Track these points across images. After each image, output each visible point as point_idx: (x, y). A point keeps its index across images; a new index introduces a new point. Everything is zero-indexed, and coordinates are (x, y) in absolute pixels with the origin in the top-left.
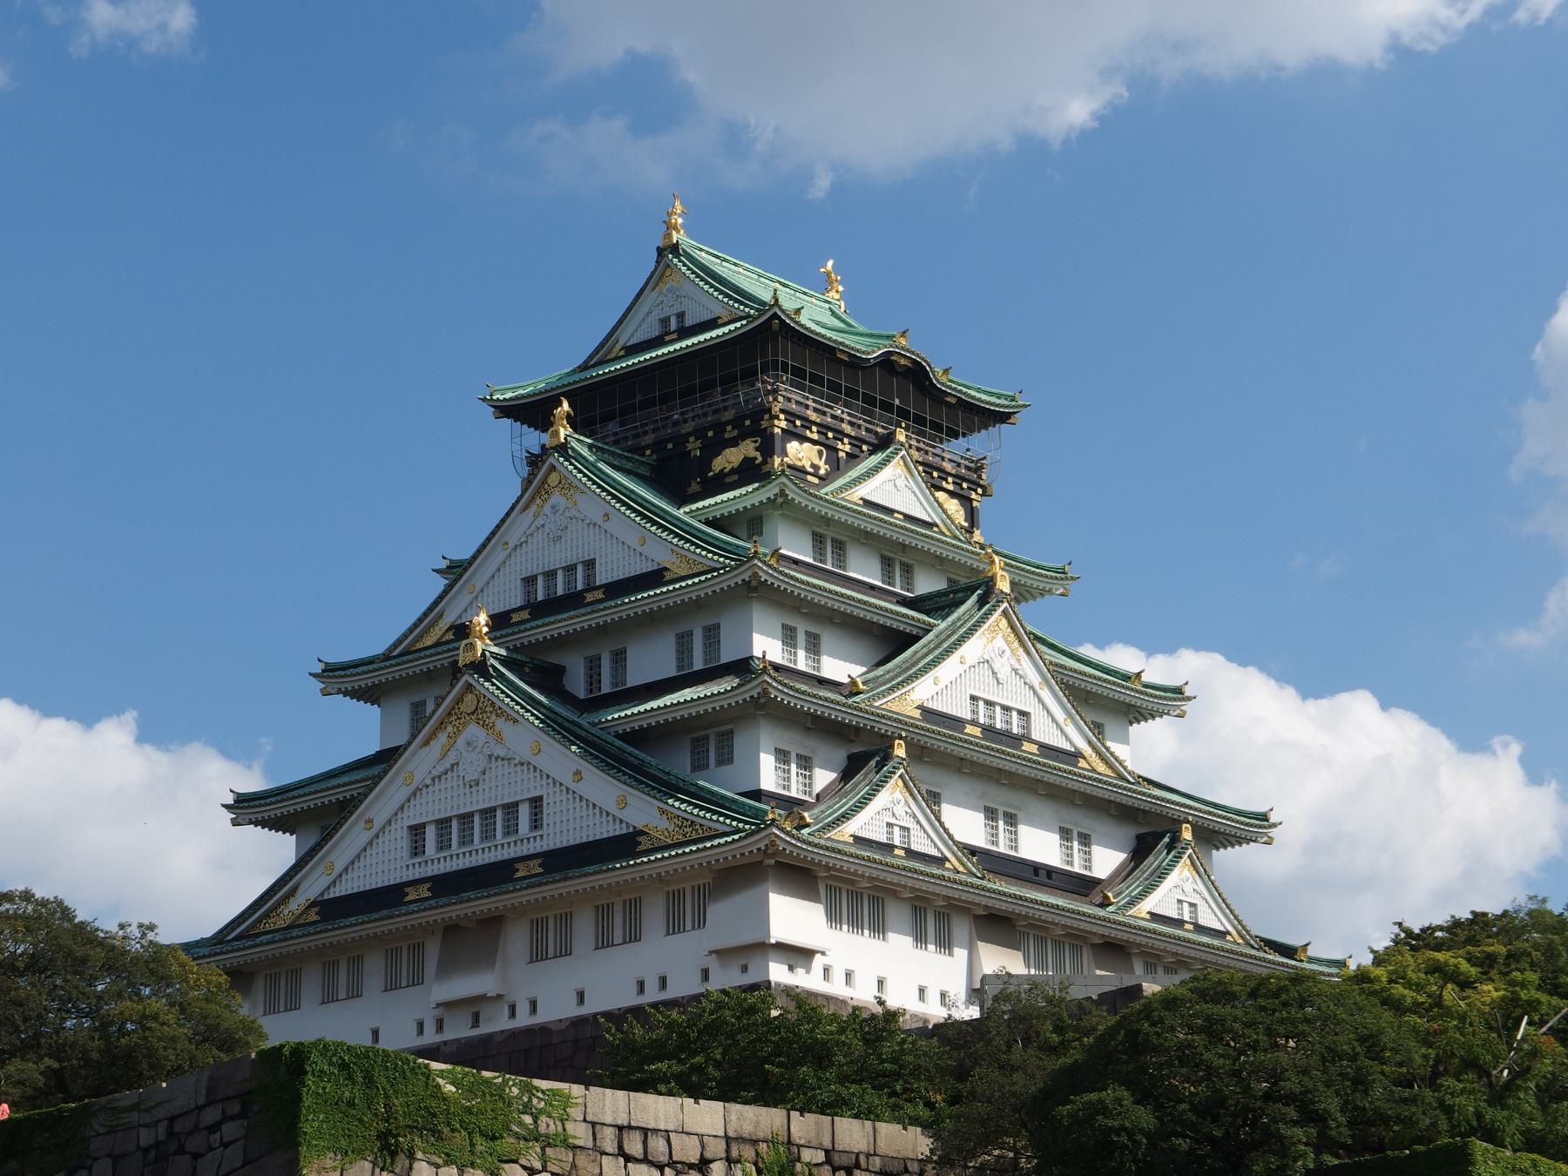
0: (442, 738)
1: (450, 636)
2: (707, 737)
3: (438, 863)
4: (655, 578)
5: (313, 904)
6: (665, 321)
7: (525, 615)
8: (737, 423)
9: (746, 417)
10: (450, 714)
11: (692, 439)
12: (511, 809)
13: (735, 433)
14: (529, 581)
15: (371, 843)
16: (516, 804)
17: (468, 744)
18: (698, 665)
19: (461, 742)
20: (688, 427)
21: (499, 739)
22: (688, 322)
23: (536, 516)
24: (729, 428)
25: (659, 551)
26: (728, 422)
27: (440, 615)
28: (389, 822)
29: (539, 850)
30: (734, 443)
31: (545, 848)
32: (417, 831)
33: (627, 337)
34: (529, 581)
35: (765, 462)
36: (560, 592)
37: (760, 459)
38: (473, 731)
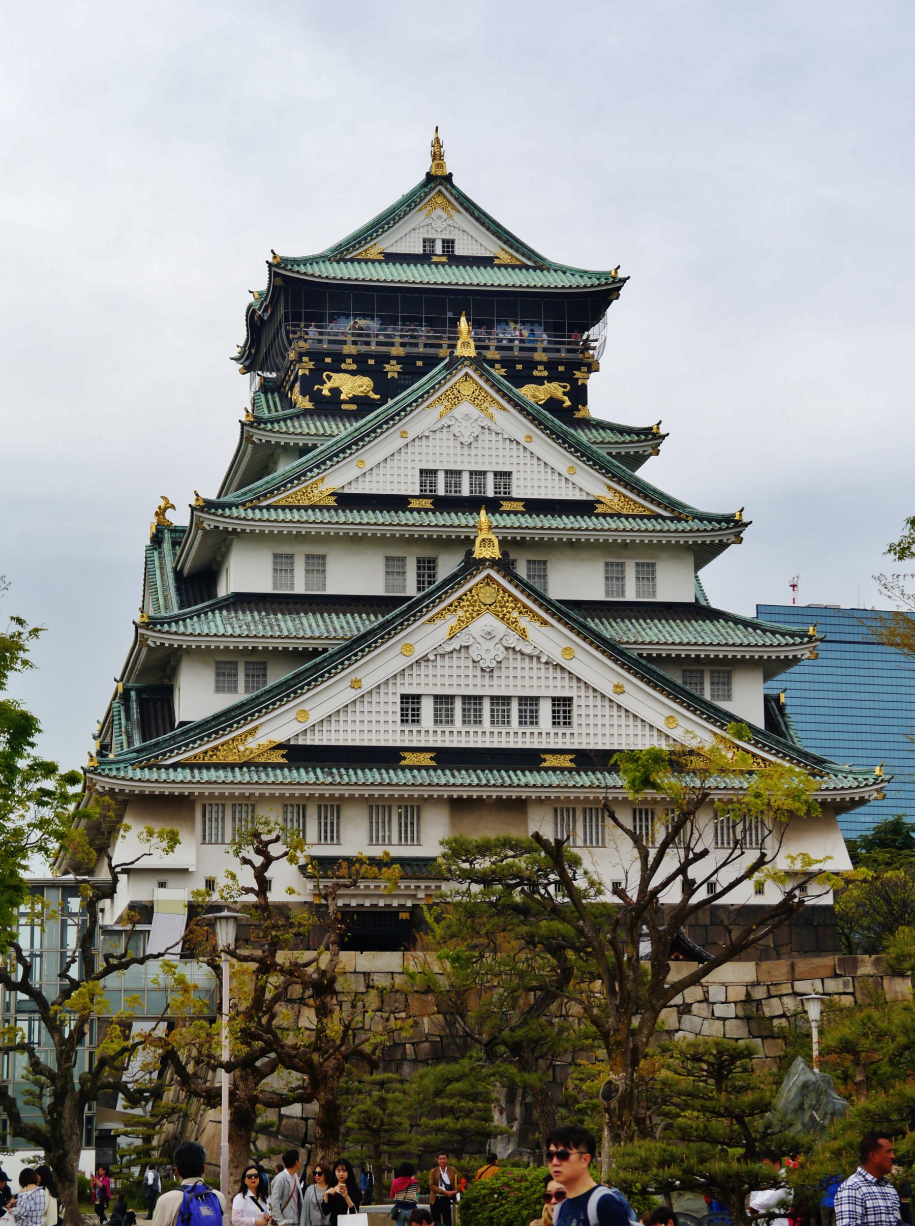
0: (452, 620)
1: (331, 502)
2: (702, 672)
3: (429, 733)
4: (585, 508)
5: (280, 746)
6: (429, 242)
7: (427, 504)
8: (550, 366)
9: (562, 364)
10: (460, 598)
11: (497, 366)
12: (530, 703)
13: (546, 373)
14: (427, 474)
15: (355, 701)
16: (535, 700)
17: (489, 633)
18: (631, 595)
20: (497, 356)
21: (523, 635)
22: (459, 251)
24: (541, 367)
26: (541, 363)
27: (323, 478)
28: (379, 687)
29: (568, 746)
30: (539, 381)
31: (576, 747)
33: (392, 242)
34: (427, 474)
35: (574, 408)
36: (465, 492)
37: (568, 403)
38: (488, 621)
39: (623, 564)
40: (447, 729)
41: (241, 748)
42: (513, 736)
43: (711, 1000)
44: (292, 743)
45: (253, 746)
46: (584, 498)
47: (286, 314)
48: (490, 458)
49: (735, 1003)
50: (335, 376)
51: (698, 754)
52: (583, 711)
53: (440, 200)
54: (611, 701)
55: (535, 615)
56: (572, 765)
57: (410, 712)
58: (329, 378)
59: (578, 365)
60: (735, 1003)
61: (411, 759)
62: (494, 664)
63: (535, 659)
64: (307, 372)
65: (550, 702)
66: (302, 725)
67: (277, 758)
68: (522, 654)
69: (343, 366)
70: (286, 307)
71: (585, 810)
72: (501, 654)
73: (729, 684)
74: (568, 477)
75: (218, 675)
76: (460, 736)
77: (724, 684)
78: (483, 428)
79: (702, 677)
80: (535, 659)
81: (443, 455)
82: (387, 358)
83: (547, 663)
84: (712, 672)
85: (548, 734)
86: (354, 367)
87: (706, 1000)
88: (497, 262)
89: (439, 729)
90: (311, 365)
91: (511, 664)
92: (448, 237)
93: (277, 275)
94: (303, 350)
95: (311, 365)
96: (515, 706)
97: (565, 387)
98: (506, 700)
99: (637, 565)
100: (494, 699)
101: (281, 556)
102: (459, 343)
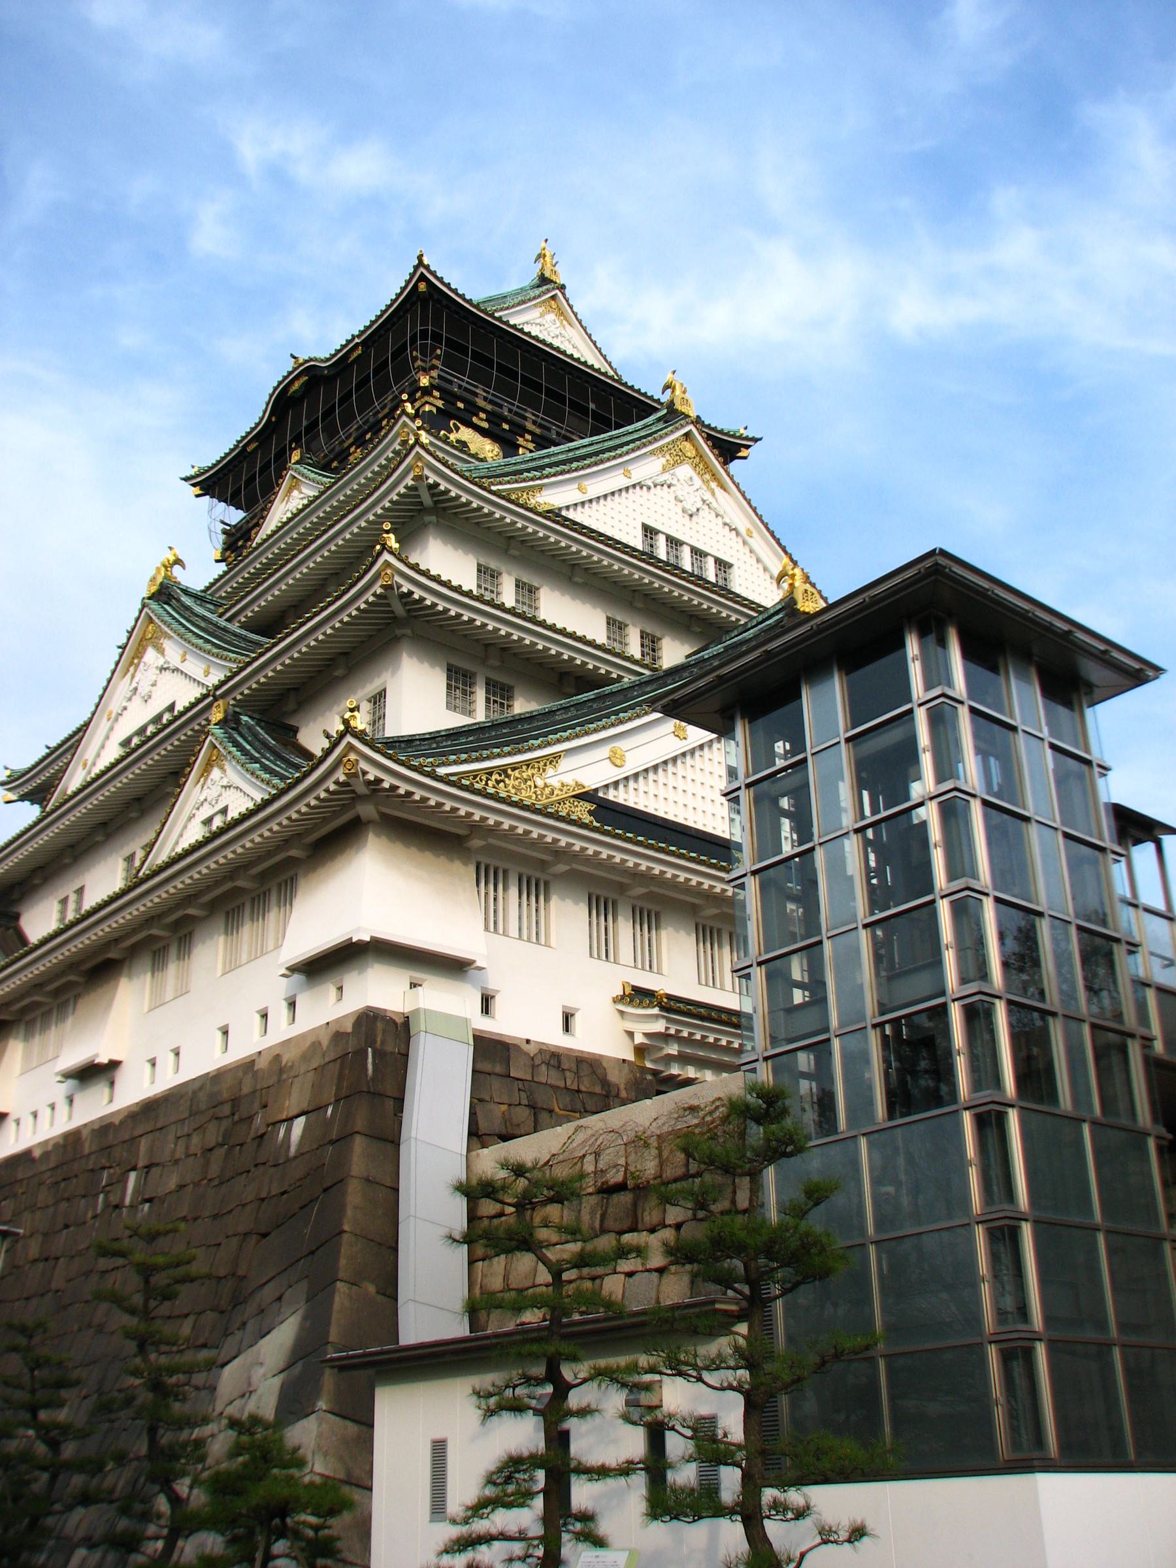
5: (587, 796)
14: (649, 532)
23: (664, 470)
34: (649, 532)
41: (540, 783)
44: (601, 794)
45: (555, 782)
50: (462, 428)
58: (457, 429)
66: (616, 771)
67: (582, 811)
69: (475, 419)
78: (704, 501)
82: (523, 431)
86: (485, 425)
93: (423, 278)
95: (440, 403)
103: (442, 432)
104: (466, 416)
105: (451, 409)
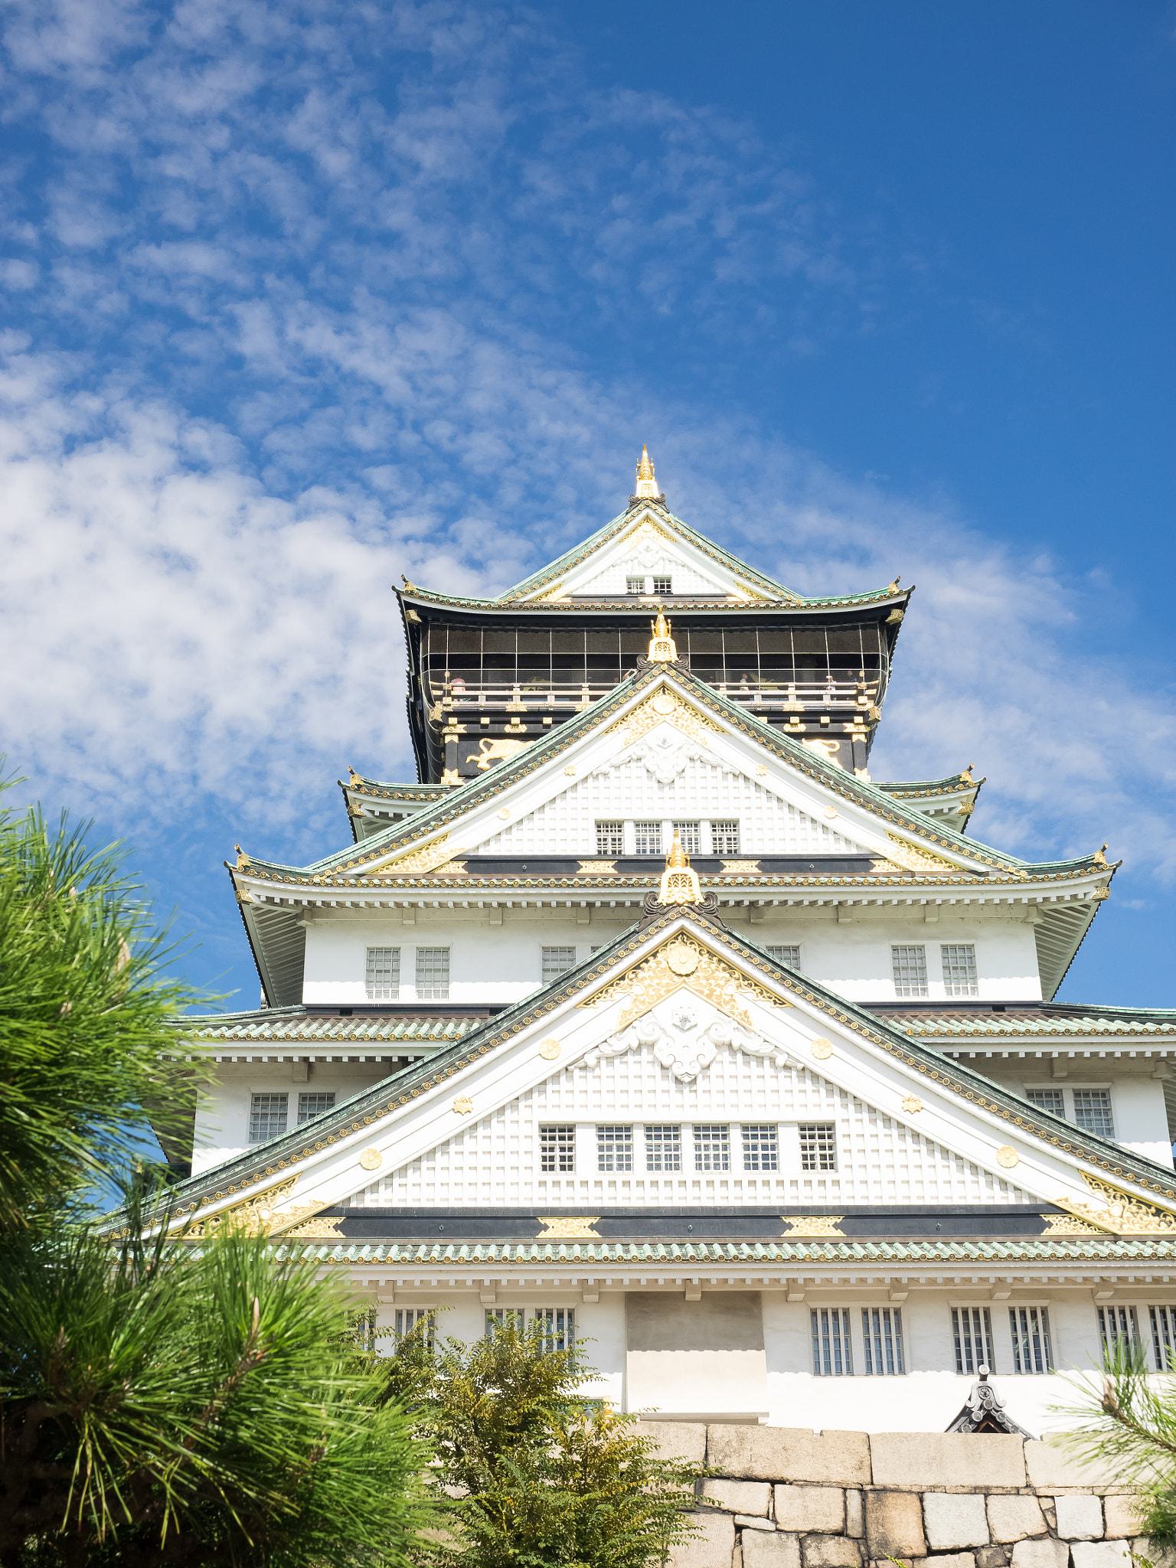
1: (458, 868)
2: (1058, 1094)
5: (328, 1212)
7: (607, 868)
9: (825, 713)
12: (761, 1132)
14: (609, 826)
15: (459, 1137)
17: (685, 1020)
19: (666, 1013)
23: (627, 745)
25: (860, 832)
27: (445, 837)
28: (501, 1110)
32: (558, 1134)
38: (685, 1001)
39: (921, 948)
40: (619, 1176)
41: (265, 1215)
42: (735, 1188)
43: (1064, 1533)
44: (353, 1205)
45: (286, 1210)
46: (853, 851)
47: (425, 659)
48: (705, 798)
49: (1128, 1538)
50: (496, 743)
51: (1065, 1212)
52: (856, 1144)
53: (647, 526)
54: (901, 1126)
55: (764, 991)
56: (839, 1233)
57: (557, 1153)
58: (489, 746)
59: (848, 715)
60: (1128, 1538)
61: (557, 1228)
62: (695, 1070)
63: (767, 1062)
64: (456, 739)
65: (796, 1131)
68: (744, 1054)
69: (508, 729)
70: (425, 651)
71: (865, 1312)
72: (710, 1052)
73: (1107, 1112)
74: (827, 823)
75: (255, 1115)
76: (642, 1189)
77: (1098, 1112)
78: (692, 759)
79: (1060, 1102)
80: (767, 1062)
81: (630, 800)
83: (786, 1067)
84: (1077, 1094)
85: (794, 1183)
86: (523, 729)
87: (1051, 1532)
88: (730, 599)
89: (606, 1176)
90: (461, 729)
91: (730, 1069)
92: (661, 572)
94: (449, 709)
95: (461, 729)
96: (736, 1137)
97: (833, 746)
98: (720, 1130)
99: (945, 948)
100: (702, 1130)
101: (380, 950)
102: (653, 643)
103: (469, 759)
104: (496, 728)
105: (476, 729)
